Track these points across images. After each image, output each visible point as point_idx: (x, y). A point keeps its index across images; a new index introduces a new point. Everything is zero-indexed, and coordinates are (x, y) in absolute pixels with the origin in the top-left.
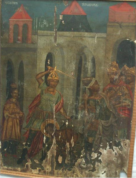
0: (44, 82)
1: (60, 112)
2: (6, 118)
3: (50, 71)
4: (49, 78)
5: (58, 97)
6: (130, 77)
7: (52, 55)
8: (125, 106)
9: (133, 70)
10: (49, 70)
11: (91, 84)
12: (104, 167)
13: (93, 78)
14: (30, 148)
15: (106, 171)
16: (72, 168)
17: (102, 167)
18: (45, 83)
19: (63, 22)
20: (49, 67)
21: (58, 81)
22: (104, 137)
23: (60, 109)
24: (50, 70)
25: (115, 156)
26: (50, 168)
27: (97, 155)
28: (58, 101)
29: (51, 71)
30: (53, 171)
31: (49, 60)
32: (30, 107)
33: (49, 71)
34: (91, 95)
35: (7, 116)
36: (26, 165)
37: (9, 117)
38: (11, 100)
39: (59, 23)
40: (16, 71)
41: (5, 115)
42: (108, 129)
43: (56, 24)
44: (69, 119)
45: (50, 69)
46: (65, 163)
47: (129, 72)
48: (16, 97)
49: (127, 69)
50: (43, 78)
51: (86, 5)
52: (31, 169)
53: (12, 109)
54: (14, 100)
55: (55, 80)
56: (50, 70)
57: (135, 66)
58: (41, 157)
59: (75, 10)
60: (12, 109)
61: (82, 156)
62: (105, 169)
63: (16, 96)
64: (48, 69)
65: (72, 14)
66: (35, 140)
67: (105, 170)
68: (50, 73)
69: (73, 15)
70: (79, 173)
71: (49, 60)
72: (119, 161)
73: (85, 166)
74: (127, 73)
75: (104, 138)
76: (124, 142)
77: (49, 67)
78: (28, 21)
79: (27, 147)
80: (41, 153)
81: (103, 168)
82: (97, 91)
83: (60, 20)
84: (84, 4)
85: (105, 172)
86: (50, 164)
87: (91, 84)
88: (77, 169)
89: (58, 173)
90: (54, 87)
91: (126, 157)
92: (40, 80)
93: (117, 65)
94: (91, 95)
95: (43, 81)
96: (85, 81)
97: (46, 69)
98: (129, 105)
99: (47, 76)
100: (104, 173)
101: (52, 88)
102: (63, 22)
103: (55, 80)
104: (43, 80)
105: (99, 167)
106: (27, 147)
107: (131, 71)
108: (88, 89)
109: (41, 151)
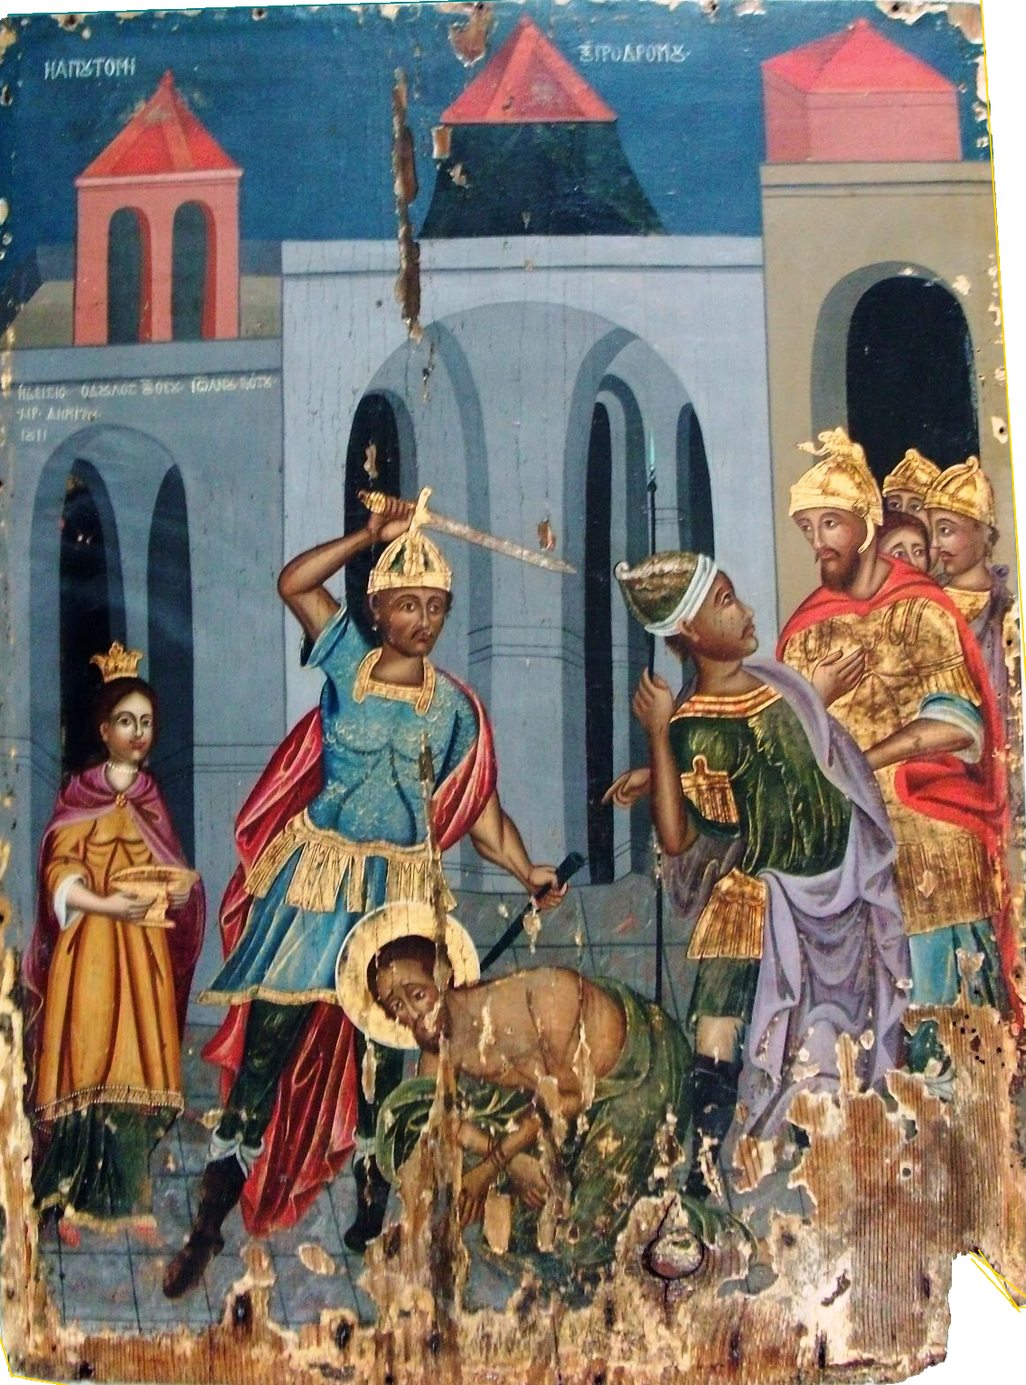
0: (343, 610)
1: (476, 840)
2: (67, 923)
3: (384, 524)
4: (379, 580)
5: (457, 719)
6: (952, 532)
7: (395, 406)
8: (942, 754)
9: (966, 483)
10: (373, 524)
11: (688, 608)
12: (831, 1249)
13: (701, 558)
14: (256, 1152)
15: (850, 1277)
16: (595, 1280)
17: (816, 1251)
18: (351, 624)
19: (456, 173)
20: (377, 502)
21: (444, 601)
22: (814, 1004)
23: (476, 812)
24: (387, 518)
25: (906, 1147)
26: (422, 1305)
27: (778, 1150)
28: (458, 748)
29: (391, 530)
30: (451, 1327)
31: (371, 451)
32: (248, 821)
33: (379, 531)
34: (695, 683)
35: (71, 907)
36: (230, 1300)
37: (88, 913)
38: (97, 775)
39: (427, 185)
40: (133, 561)
41: (60, 907)
42: (833, 937)
43: (412, 190)
44: (548, 886)
45: (382, 515)
46: (533, 1250)
47: (945, 500)
48: (139, 748)
49: (924, 478)
50: (337, 585)
51: (609, 55)
52: (271, 1325)
53: (110, 848)
54: (121, 775)
55: (424, 596)
56: (387, 518)
57: (977, 453)
58: (346, 1220)
59: (535, 89)
60: (110, 848)
61: (660, 1172)
62: (845, 1263)
63: (134, 743)
64: (368, 514)
65: (516, 120)
66: (294, 1087)
67: (839, 1273)
68: (383, 545)
69: (528, 125)
70: (651, 1314)
71: (371, 451)
72: (940, 1185)
73: (689, 1256)
74: (929, 512)
75: (818, 1009)
76: (960, 1025)
77: (377, 502)
78: (214, 183)
79: (236, 1150)
80: (351, 1183)
81: (828, 1256)
82: (729, 651)
83: (439, 161)
84: (593, 51)
85: (843, 1284)
86: (418, 1268)
87: (688, 608)
88: (628, 1287)
89: (488, 1336)
90: (420, 647)
91: (983, 1146)
92: (312, 604)
93: (857, 451)
94: (695, 683)
95: (339, 606)
96: (640, 581)
97: (356, 516)
98: (966, 743)
99: (360, 565)
100: (840, 1292)
101: (406, 653)
102: (456, 173)
103: (424, 596)
104: (333, 604)
105: (794, 1253)
106: (235, 1147)
107: (951, 488)
108: (670, 641)
109: (347, 1167)
